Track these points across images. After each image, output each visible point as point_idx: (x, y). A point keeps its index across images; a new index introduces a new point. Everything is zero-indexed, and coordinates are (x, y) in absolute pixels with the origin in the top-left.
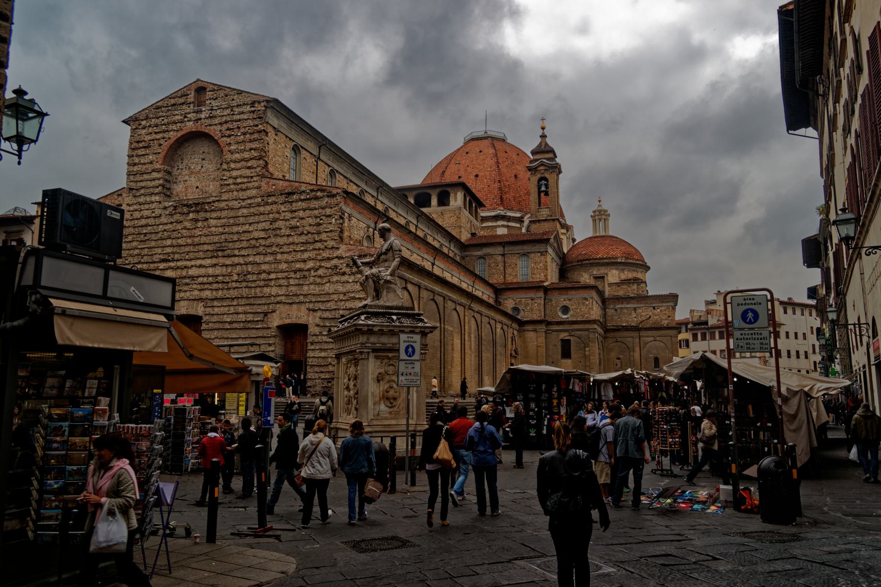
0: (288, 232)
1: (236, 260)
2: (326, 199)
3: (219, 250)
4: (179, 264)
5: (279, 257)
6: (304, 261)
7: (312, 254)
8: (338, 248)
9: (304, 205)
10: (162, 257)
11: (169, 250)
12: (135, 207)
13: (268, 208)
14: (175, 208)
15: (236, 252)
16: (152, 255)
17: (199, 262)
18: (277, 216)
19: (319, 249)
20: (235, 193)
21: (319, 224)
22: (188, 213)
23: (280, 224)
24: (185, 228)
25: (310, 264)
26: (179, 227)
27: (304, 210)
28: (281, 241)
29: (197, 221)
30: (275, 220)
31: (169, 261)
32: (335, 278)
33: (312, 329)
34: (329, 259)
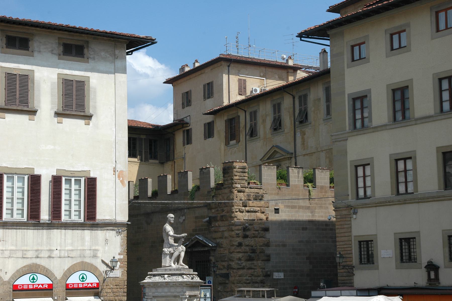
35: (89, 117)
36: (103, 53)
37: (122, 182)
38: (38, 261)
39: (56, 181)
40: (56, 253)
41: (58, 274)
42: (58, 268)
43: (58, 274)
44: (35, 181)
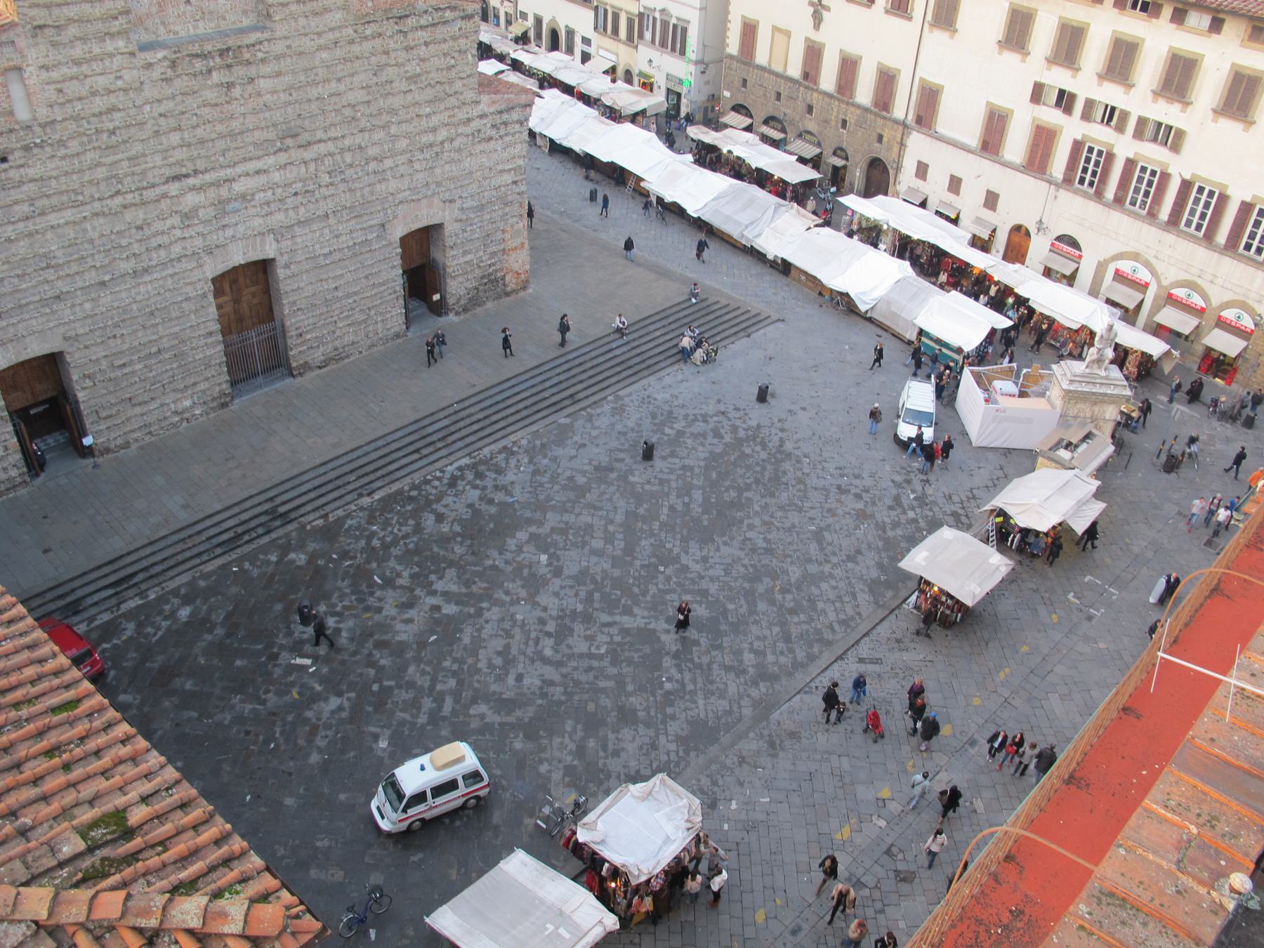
0: (404, 86)
1: (322, 148)
2: (459, 23)
3: (290, 136)
4: (208, 177)
5: (394, 129)
6: (434, 130)
7: (444, 117)
8: (478, 103)
9: (423, 35)
10: (168, 172)
11: (179, 155)
12: (65, 70)
13: (368, 46)
14: (173, 65)
15: (320, 135)
16: (144, 173)
17: (252, 166)
18: (384, 59)
19: (453, 108)
20: (302, 21)
21: (450, 68)
22: (210, 71)
23: (391, 72)
24: (205, 104)
25: (443, 134)
26: (192, 103)
27: (426, 44)
28: (396, 102)
29: (230, 86)
30: (382, 67)
31: (187, 176)
32: (479, 148)
33: (450, 228)
34: (469, 120)
38: (1199, 281)
39: (1246, 208)
40: (1219, 281)
41: (1215, 302)
43: (1215, 302)
44: (1223, 199)
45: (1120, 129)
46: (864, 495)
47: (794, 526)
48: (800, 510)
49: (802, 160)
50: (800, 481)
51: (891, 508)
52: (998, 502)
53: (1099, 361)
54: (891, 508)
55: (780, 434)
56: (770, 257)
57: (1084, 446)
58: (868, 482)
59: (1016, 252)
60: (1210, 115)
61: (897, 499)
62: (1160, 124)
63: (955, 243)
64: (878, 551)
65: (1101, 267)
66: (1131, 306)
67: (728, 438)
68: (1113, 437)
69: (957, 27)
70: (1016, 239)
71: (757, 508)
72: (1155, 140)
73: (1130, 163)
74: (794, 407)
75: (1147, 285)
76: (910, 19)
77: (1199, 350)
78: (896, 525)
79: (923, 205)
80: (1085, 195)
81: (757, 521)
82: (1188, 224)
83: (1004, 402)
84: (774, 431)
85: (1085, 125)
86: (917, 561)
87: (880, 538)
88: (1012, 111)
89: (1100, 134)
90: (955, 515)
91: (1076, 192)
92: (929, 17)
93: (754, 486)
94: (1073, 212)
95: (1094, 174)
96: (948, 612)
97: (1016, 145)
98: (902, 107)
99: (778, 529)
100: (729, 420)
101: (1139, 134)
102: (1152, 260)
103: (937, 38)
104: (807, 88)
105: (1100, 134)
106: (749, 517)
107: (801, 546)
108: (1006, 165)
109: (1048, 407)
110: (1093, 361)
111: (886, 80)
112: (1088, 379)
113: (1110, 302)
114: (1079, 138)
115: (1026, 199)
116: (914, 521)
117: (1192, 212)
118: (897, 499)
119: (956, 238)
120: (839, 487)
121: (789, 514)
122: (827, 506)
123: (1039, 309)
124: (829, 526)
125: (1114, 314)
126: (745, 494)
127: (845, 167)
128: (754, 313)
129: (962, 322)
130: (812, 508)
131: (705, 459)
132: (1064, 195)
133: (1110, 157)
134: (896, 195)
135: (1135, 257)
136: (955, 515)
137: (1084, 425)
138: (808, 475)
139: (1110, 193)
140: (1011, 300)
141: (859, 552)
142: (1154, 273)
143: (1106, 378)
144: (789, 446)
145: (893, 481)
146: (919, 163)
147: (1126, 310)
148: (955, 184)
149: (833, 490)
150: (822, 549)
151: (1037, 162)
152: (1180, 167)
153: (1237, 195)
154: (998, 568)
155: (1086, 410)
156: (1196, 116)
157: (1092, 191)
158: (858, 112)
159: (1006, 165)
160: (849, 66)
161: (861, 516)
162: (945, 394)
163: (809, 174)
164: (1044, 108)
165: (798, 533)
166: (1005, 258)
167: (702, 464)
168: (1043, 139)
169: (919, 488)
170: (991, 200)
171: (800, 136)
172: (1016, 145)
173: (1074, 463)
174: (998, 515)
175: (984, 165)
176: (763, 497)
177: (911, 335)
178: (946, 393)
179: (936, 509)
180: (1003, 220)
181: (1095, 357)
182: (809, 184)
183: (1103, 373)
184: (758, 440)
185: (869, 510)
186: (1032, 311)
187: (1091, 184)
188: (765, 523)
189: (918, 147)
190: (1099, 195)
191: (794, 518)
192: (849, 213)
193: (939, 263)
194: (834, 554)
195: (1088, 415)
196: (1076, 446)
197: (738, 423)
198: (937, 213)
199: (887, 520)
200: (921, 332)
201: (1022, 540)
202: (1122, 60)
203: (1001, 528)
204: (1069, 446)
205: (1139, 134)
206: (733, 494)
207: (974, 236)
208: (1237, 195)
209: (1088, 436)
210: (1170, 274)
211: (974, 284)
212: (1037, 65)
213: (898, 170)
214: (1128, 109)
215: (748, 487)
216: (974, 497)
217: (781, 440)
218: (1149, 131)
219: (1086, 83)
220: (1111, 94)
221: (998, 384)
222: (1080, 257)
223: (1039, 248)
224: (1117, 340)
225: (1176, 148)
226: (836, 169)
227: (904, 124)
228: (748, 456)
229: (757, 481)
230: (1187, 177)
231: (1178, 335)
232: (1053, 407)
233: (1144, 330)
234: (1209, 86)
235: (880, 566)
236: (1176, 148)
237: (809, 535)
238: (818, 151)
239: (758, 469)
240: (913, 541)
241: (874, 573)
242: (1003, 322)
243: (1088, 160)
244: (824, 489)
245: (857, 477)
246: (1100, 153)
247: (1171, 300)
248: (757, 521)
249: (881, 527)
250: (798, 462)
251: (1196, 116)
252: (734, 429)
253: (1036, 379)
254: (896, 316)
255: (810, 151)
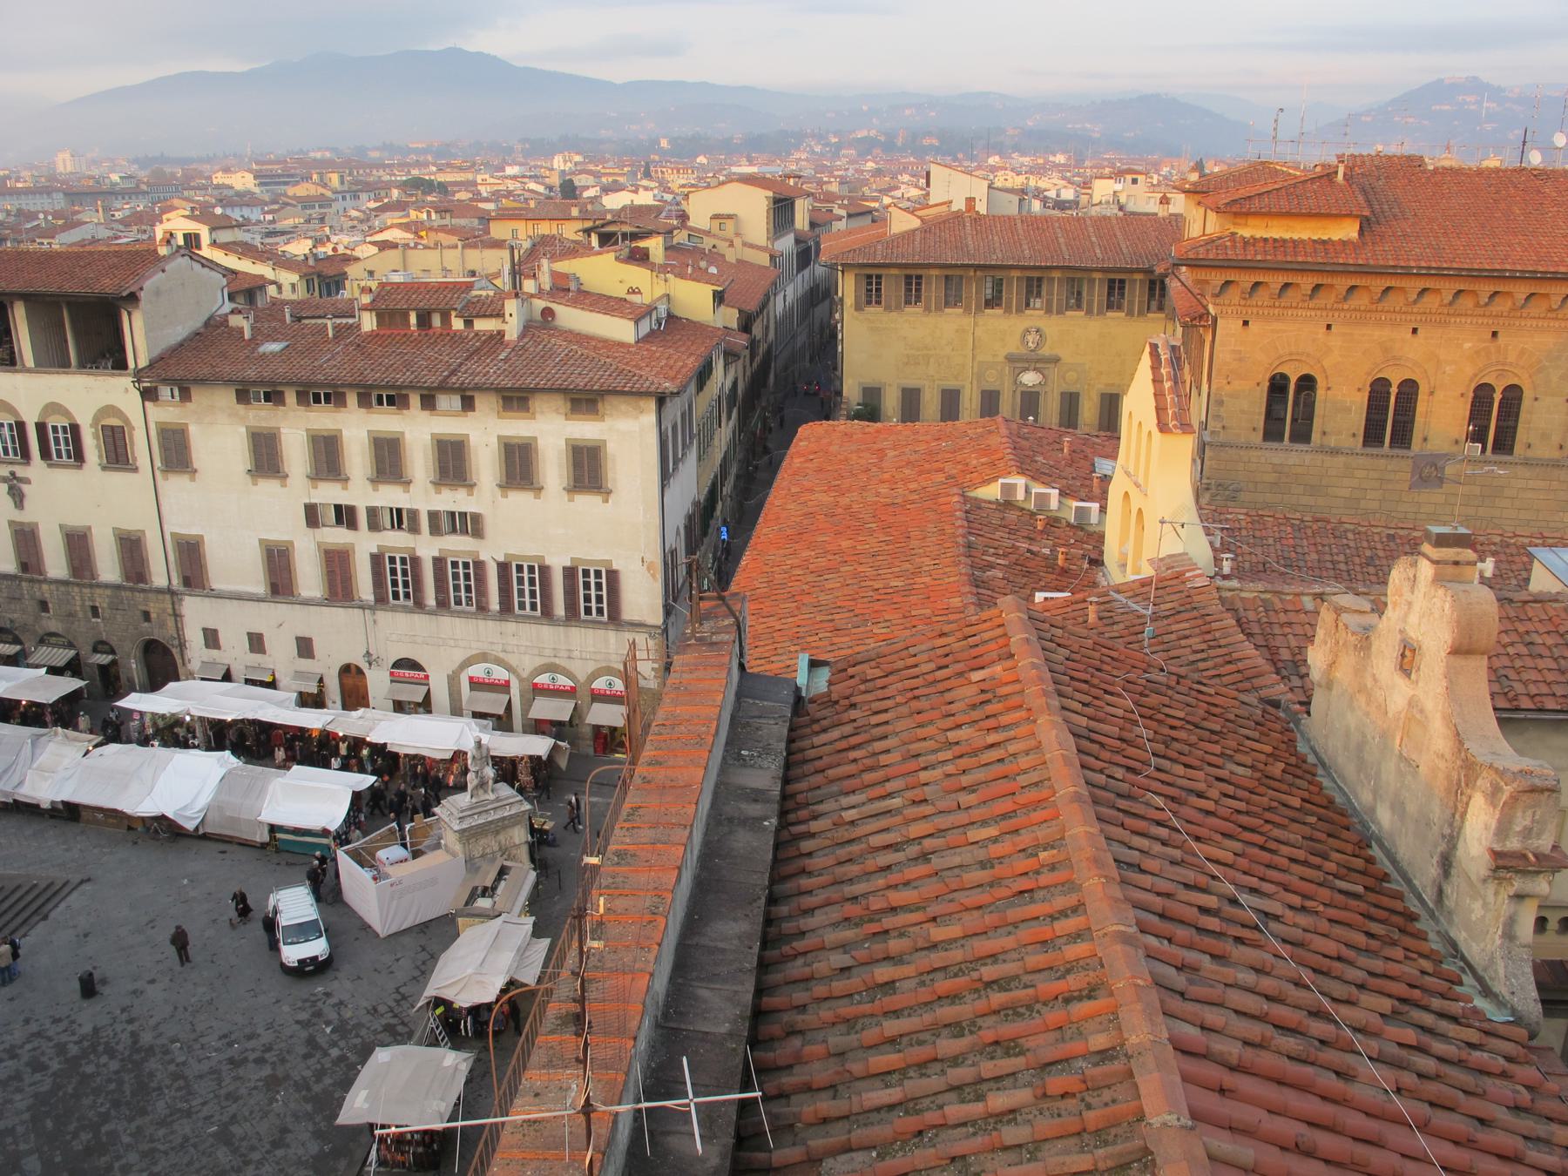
35: (609, 492)
36: (623, 407)
37: (653, 576)
38: (557, 661)
39: (569, 573)
40: (576, 654)
41: (582, 677)
42: (582, 670)
43: (582, 677)
44: (545, 570)
45: (414, 529)
46: (267, 1056)
47: (186, 1139)
48: (188, 1114)
49: (54, 671)
50: (176, 1077)
51: (306, 1057)
52: (430, 991)
53: (482, 785)
54: (306, 1057)
55: (130, 1028)
56: (46, 805)
57: (503, 883)
58: (267, 1037)
59: (354, 697)
60: (498, 491)
61: (311, 1042)
62: (453, 514)
63: (279, 710)
64: (309, 1117)
65: (453, 680)
66: (501, 712)
67: (55, 1066)
68: (533, 860)
69: (196, 465)
70: (349, 681)
71: (126, 1139)
72: (454, 531)
73: (439, 562)
74: (139, 985)
75: (507, 683)
76: (136, 470)
77: (587, 731)
78: (319, 1075)
79: (227, 677)
80: (406, 609)
81: (132, 1157)
82: (522, 606)
83: (396, 872)
84: (118, 1028)
85: (376, 535)
86: (357, 1107)
87: (306, 1100)
88: (291, 543)
89: (396, 540)
90: (389, 1029)
91: (394, 609)
92: (158, 463)
93: (113, 1112)
94: (400, 631)
95: (406, 584)
96: (420, 1150)
97: (309, 577)
98: (161, 572)
99: (166, 1153)
100: (50, 1039)
101: (435, 530)
102: (501, 655)
103: (175, 486)
104: (31, 581)
105: (396, 540)
106: (118, 1158)
107: (204, 1160)
108: (307, 603)
109: (449, 857)
110: (476, 788)
111: (131, 546)
112: (477, 809)
113: (476, 715)
114: (375, 550)
115: (342, 636)
116: (342, 1058)
117: (521, 593)
118: (311, 1042)
119: (280, 704)
120: (231, 1061)
121: (176, 1126)
122: (223, 1092)
123: (402, 751)
124: (234, 1117)
125: (485, 727)
126: (104, 1129)
127: (114, 663)
128: (43, 885)
129: (315, 799)
130: (204, 1104)
131: (29, 1109)
132: (382, 616)
133: (416, 561)
134: (191, 676)
135: (483, 657)
136: (389, 1029)
137: (494, 860)
138: (184, 1064)
139: (431, 601)
140: (365, 752)
141: (285, 1130)
142: (509, 668)
143: (498, 800)
144: (146, 1038)
145: (298, 1022)
146: (205, 630)
147: (499, 717)
148: (256, 642)
149: (225, 1067)
150: (235, 1151)
151: (339, 588)
152: (491, 551)
153: (557, 562)
154: (456, 1069)
155: (491, 843)
156: (484, 494)
157: (411, 603)
158: (108, 592)
159: (307, 603)
160: (78, 543)
161: (273, 1083)
162: (323, 890)
163: (70, 684)
164: (325, 529)
165: (195, 1146)
166: (345, 707)
167: (26, 1116)
168: (337, 564)
169: (333, 1016)
170: (305, 647)
171: (42, 641)
172: (309, 577)
173: (498, 907)
174: (436, 1006)
175: (281, 611)
176: (131, 1120)
177: (263, 836)
178: (325, 886)
179: (363, 1032)
180: (327, 663)
181: (476, 782)
182: (72, 698)
183: (492, 796)
184: (101, 1048)
185: (280, 1072)
186: (395, 756)
187: (407, 596)
188: (144, 1155)
189: (196, 613)
190: (419, 605)
191: (184, 1127)
192: (137, 716)
193: (269, 738)
194: (253, 1148)
195: (496, 848)
196: (494, 888)
197: (64, 1038)
198: (248, 681)
199: (308, 1073)
200: (273, 829)
201: (475, 1022)
202: (388, 460)
203: (447, 1019)
204: (487, 892)
205: (435, 530)
206: (85, 1136)
207: (301, 694)
208: (557, 562)
209: (503, 872)
210: (527, 664)
211: (315, 750)
212: (298, 486)
213: (182, 646)
214: (415, 507)
215: (105, 1118)
216: (404, 998)
217: (134, 1035)
218: (445, 523)
219: (360, 493)
220: (390, 497)
221: (382, 854)
222: (427, 677)
223: (378, 682)
224: (493, 753)
225: (478, 533)
226: (104, 669)
227: (170, 591)
228: (92, 1076)
229: (116, 1104)
230: (501, 559)
231: (560, 724)
232: (454, 855)
233: (525, 732)
234: (485, 463)
235: (318, 1135)
236: (478, 533)
237: (211, 1140)
238: (72, 653)
239: (113, 1086)
240: (347, 1084)
241: (314, 1148)
242: (366, 781)
243: (394, 572)
244: (213, 1071)
245: (250, 1037)
246: (403, 561)
247: (538, 690)
248: (132, 1157)
249: (302, 1086)
250: (167, 1052)
251: (484, 494)
252: (61, 1049)
253: (425, 831)
254: (234, 821)
255: (62, 656)
